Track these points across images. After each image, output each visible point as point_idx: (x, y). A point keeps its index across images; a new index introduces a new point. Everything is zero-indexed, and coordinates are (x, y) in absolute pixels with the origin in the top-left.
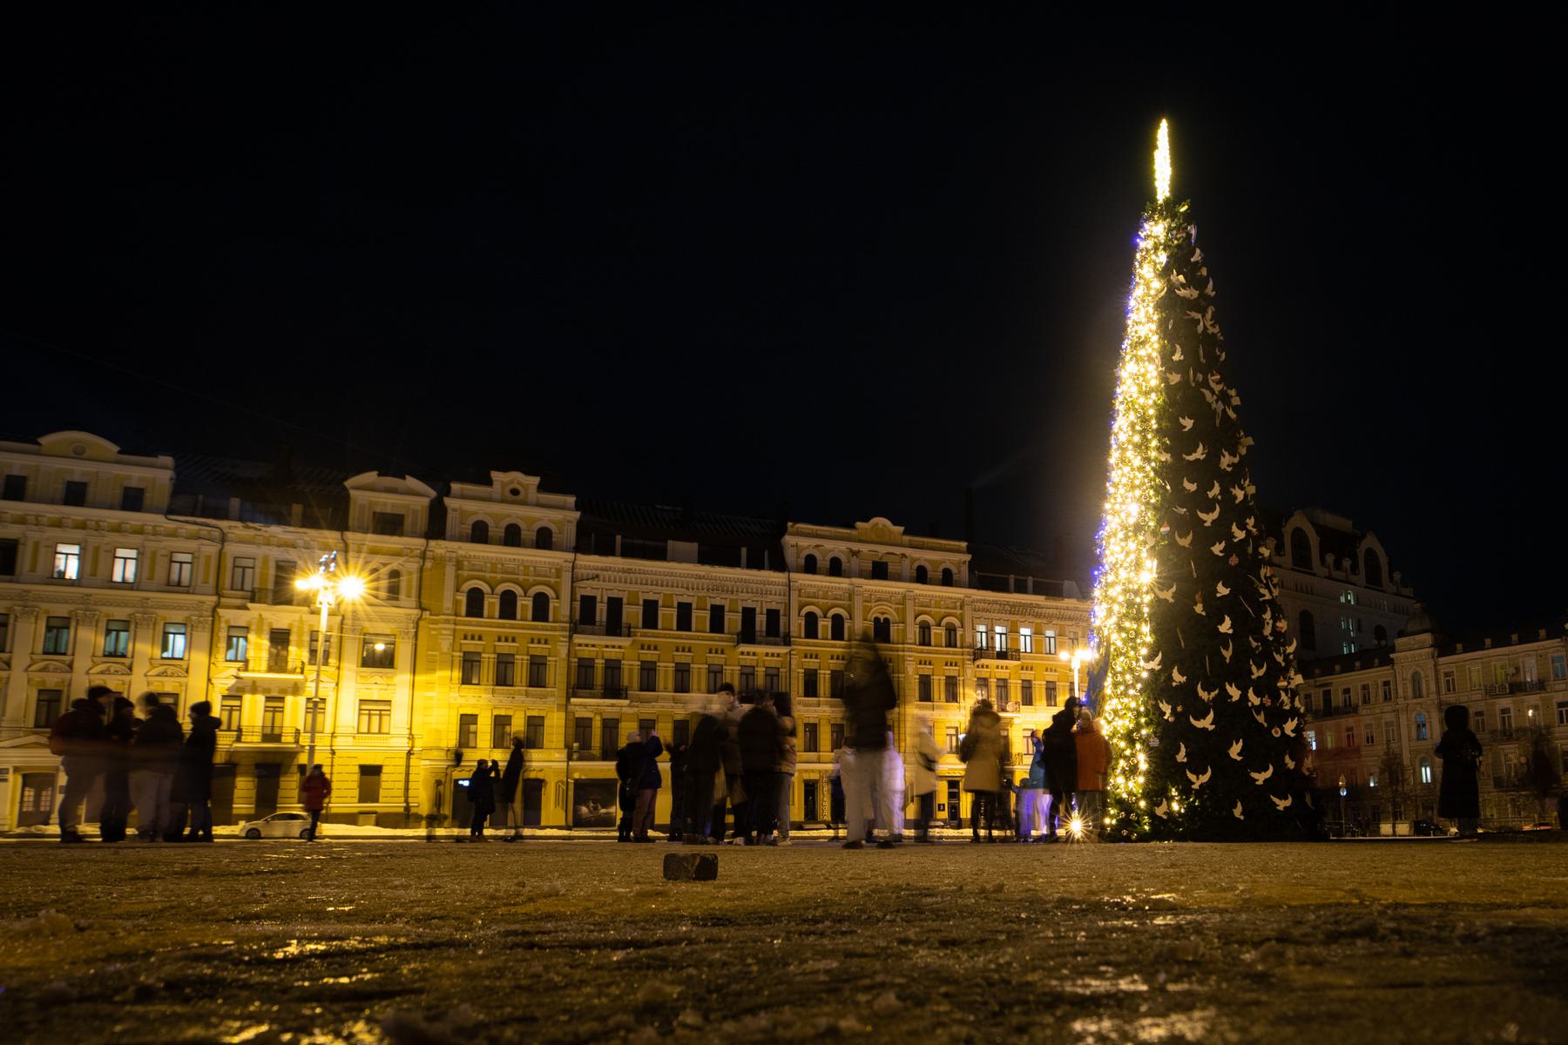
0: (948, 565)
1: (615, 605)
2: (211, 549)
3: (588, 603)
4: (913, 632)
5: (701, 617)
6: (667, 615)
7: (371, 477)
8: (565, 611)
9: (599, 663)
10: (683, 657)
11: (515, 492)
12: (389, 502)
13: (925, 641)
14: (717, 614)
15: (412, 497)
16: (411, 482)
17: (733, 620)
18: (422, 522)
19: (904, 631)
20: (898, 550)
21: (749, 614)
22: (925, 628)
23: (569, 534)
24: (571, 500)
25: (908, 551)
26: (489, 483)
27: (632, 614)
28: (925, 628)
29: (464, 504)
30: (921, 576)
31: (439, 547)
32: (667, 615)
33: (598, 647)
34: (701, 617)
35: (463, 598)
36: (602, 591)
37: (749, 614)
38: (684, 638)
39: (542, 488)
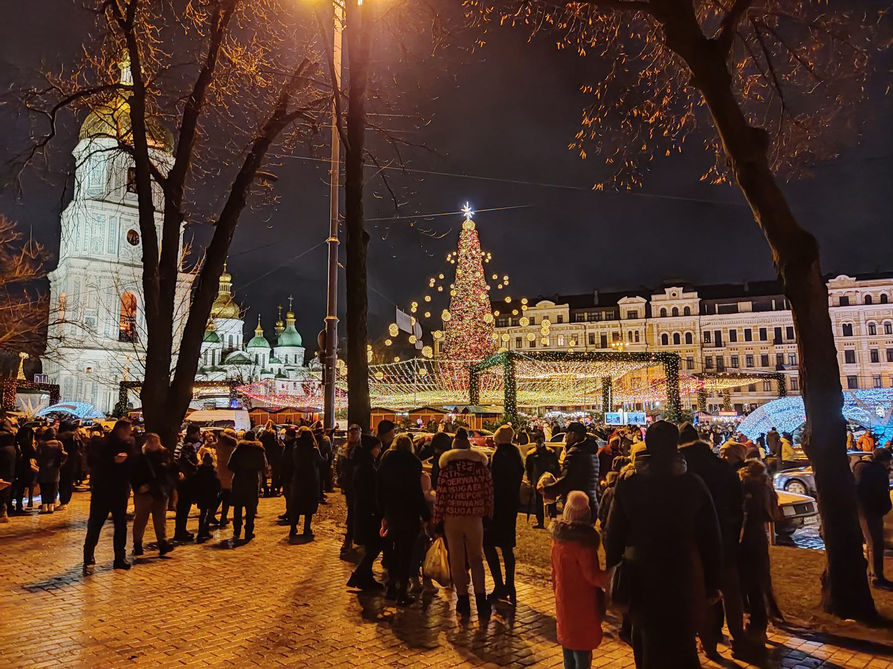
0: (884, 292)
1: (718, 334)
2: (582, 332)
3: (707, 334)
4: (865, 329)
5: (756, 334)
6: (741, 335)
7: (625, 299)
8: (698, 339)
9: (714, 358)
10: (750, 352)
11: (674, 295)
12: (632, 307)
13: (873, 333)
14: (763, 334)
15: (637, 303)
16: (638, 298)
17: (771, 334)
18: (644, 314)
19: (860, 329)
20: (854, 290)
21: (778, 331)
22: (872, 326)
23: (695, 309)
24: (696, 294)
25: (858, 289)
26: (665, 293)
27: (725, 337)
28: (872, 326)
29: (659, 302)
30: (868, 301)
31: (650, 321)
32: (741, 335)
33: (713, 352)
34: (756, 334)
35: (661, 338)
36: (712, 329)
37: (778, 331)
38: (749, 344)
39: (684, 292)
